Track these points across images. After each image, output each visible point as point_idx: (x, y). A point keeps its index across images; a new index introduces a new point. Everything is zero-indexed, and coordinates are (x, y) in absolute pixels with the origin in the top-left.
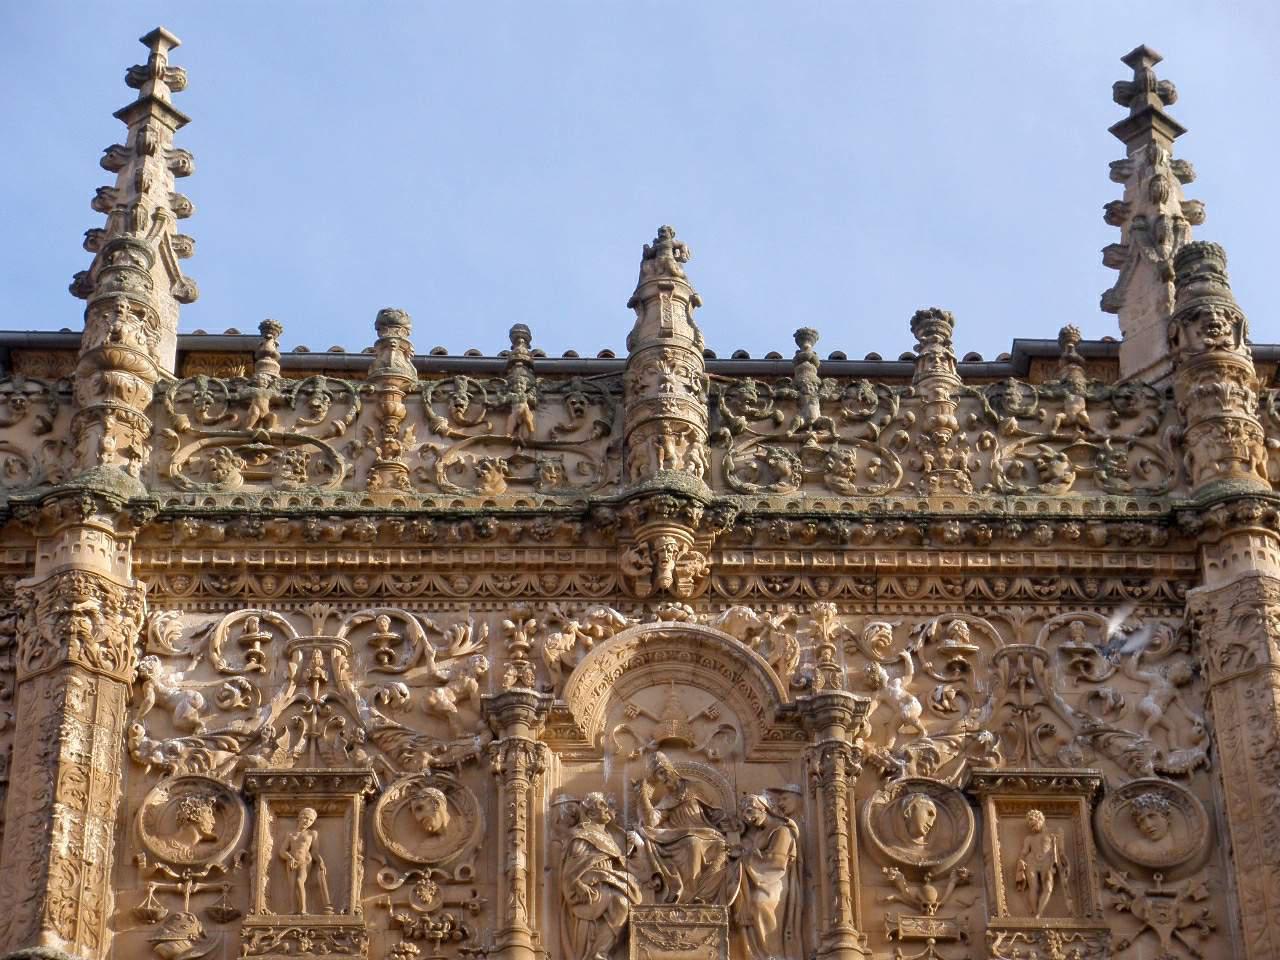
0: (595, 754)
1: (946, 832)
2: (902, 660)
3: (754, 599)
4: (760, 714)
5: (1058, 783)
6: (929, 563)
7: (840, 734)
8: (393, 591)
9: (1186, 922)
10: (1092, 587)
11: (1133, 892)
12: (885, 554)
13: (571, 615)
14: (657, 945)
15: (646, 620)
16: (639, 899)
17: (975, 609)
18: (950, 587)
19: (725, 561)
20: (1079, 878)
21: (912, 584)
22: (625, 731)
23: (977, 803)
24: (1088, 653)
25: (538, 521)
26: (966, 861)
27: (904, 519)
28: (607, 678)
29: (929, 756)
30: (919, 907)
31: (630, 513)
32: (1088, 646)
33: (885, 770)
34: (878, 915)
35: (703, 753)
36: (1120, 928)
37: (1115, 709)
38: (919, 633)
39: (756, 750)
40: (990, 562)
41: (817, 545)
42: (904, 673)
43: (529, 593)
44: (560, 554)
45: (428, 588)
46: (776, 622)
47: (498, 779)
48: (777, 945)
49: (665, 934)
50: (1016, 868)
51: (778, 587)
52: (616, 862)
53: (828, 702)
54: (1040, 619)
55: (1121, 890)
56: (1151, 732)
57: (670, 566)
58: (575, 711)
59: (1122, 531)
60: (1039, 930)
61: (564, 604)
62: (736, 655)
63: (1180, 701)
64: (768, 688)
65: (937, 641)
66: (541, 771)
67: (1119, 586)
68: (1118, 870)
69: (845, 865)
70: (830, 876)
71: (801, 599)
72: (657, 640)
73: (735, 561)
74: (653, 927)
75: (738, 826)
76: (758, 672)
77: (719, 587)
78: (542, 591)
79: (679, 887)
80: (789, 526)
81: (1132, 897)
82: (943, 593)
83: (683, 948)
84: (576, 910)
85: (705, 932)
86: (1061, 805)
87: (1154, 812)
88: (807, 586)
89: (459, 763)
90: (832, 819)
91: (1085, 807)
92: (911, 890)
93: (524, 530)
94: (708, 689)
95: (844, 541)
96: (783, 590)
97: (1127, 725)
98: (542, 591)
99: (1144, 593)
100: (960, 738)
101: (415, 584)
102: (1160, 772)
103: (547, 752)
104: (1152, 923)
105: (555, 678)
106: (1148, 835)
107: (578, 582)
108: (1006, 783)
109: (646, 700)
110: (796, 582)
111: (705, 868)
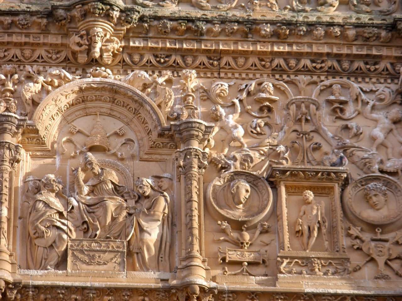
0: (51, 153)
1: (256, 203)
2: (234, 104)
3: (148, 67)
4: (149, 133)
5: (322, 175)
6: (251, 49)
7: (195, 145)
9: (394, 256)
10: (346, 65)
11: (364, 238)
12: (226, 42)
13: (39, 73)
14: (84, 262)
15: (83, 76)
16: (74, 236)
17: (277, 76)
18: (263, 63)
19: (132, 44)
20: (332, 230)
21: (241, 61)
22: (69, 141)
23: (274, 186)
24: (344, 103)
25: (21, 17)
26: (267, 219)
27: (238, 22)
28: (60, 110)
29: (247, 159)
30: (239, 244)
31: (76, 13)
32: (343, 98)
33: (222, 166)
34: (214, 248)
35: (115, 155)
36: (356, 259)
37: (357, 135)
38: (244, 89)
39: (146, 154)
40: (287, 49)
41: (186, 36)
42: (234, 112)
43: (15, 59)
44: (33, 37)
46: (161, 80)
48: (154, 264)
50: (296, 223)
51: (162, 60)
52: (61, 214)
53: (189, 125)
54: (315, 83)
55: (357, 237)
56: (377, 148)
57: (99, 45)
58: (40, 127)
59: (365, 33)
60: (308, 258)
61: (35, 66)
62: (136, 98)
63: (395, 131)
64: (154, 117)
65: (254, 94)
66: (18, 161)
67: (362, 65)
68: (355, 226)
69: (196, 219)
70: (187, 225)
71: (176, 68)
72: (90, 89)
73: (137, 44)
74: (82, 252)
76: (149, 108)
77: (127, 59)
78: (22, 59)
79: (98, 229)
80: (170, 24)
81: (363, 241)
82: (259, 66)
83: (99, 264)
84: (37, 242)
86: (324, 188)
87: (378, 193)
88: (179, 60)
90: (189, 192)
91: (337, 189)
92: (234, 235)
93: (13, 22)
95: (202, 34)
96: (165, 62)
97: (364, 144)
98: (22, 59)
99: (376, 70)
100: (266, 149)
102: (381, 171)
103: (22, 151)
104: (374, 256)
105: (29, 109)
106: (374, 206)
107: (44, 54)
108: (292, 175)
109: (82, 124)
110: (173, 58)
111: (113, 219)
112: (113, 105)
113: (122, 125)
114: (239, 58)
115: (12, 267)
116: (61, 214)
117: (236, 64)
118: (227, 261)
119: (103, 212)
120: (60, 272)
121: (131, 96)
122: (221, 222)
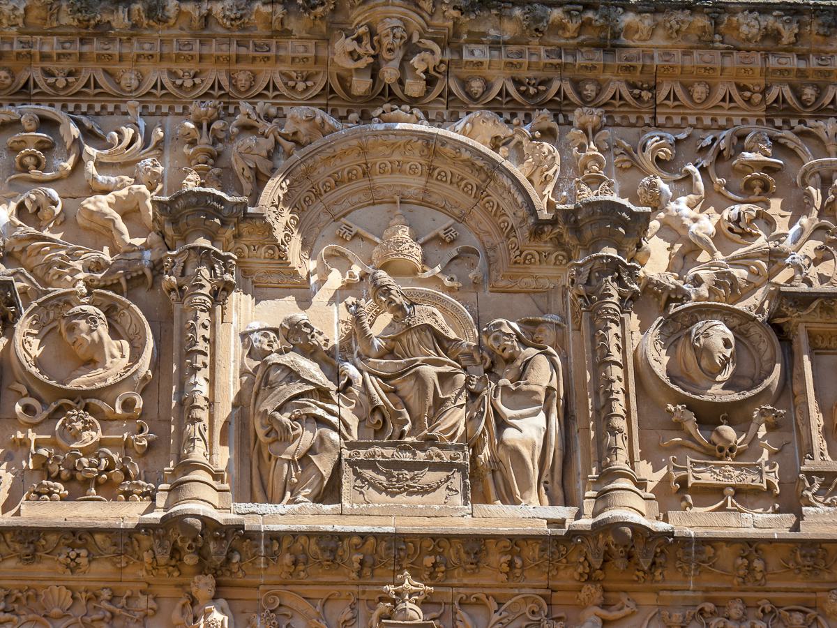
2: (689, 177)
8: (45, 88)
14: (379, 489)
30: (717, 452)
38: (709, 147)
43: (216, 93)
44: (255, 45)
45: (87, 85)
47: (173, 296)
49: (389, 476)
51: (532, 90)
62: (479, 163)
64: (520, 199)
65: (732, 157)
70: (597, 412)
71: (560, 107)
75: (482, 358)
79: (406, 422)
85: (442, 475)
88: (568, 88)
89: (123, 281)
94: (443, 209)
96: (538, 93)
98: (233, 92)
101: (71, 79)
112: (430, 181)
113: (452, 221)
114: (696, 84)
115: (220, 498)
116: (323, 394)
117: (691, 97)
118: (690, 485)
119: (416, 387)
120: (327, 508)
121: (468, 160)
122: (675, 406)
